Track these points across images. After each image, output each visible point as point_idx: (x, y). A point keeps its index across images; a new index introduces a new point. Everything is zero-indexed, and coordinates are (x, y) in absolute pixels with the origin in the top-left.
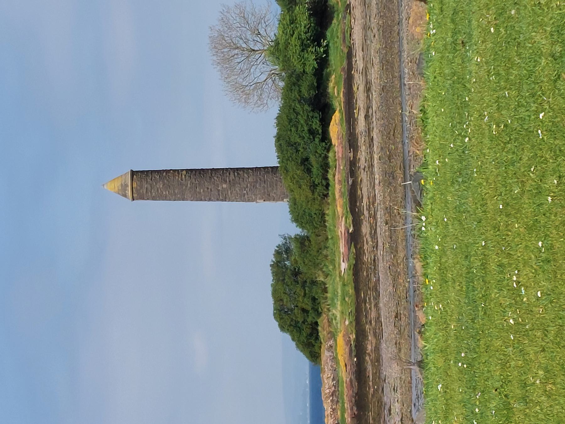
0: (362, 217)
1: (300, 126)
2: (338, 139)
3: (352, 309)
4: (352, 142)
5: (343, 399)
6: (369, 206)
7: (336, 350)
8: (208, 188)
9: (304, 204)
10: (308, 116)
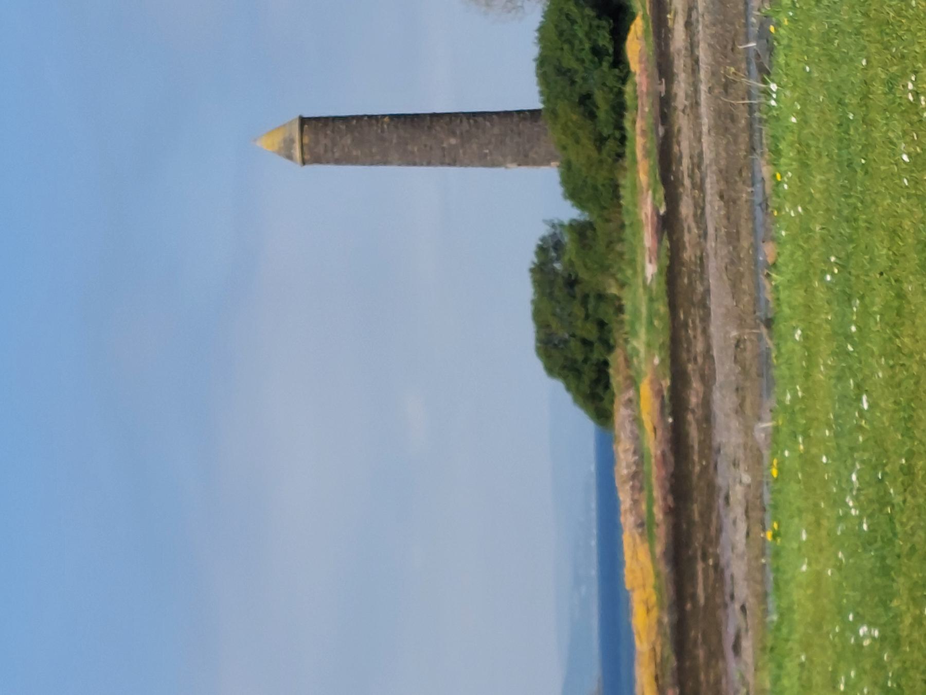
0: (681, 190)
1: (577, 42)
2: (640, 62)
3: (664, 338)
4: (663, 66)
5: (650, 486)
6: (693, 170)
7: (638, 404)
8: (426, 146)
9: (584, 169)
10: (591, 26)
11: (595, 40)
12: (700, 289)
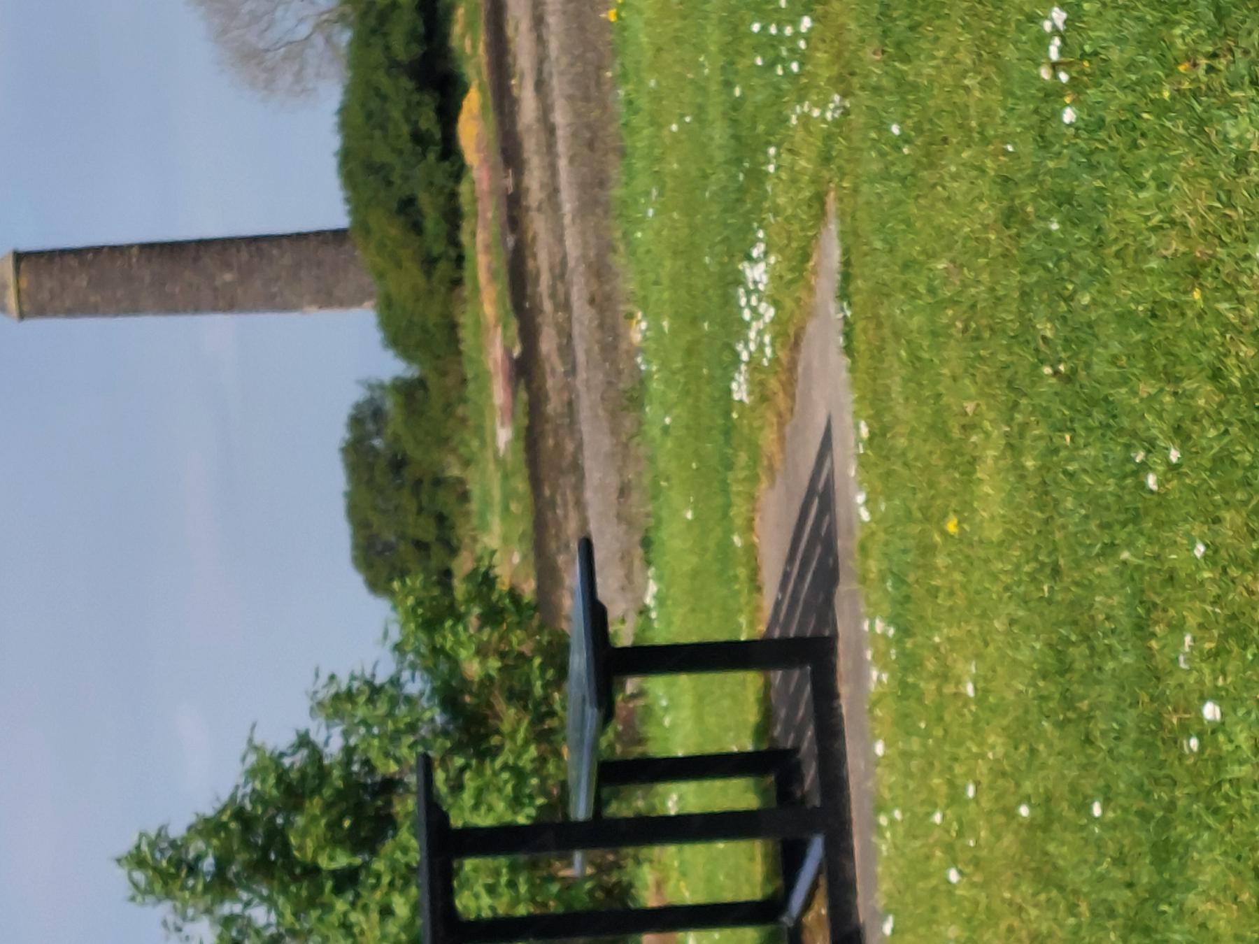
2: (478, 150)
3: (524, 525)
4: (509, 153)
10: (409, 103)
11: (416, 122)
12: (570, 447)
